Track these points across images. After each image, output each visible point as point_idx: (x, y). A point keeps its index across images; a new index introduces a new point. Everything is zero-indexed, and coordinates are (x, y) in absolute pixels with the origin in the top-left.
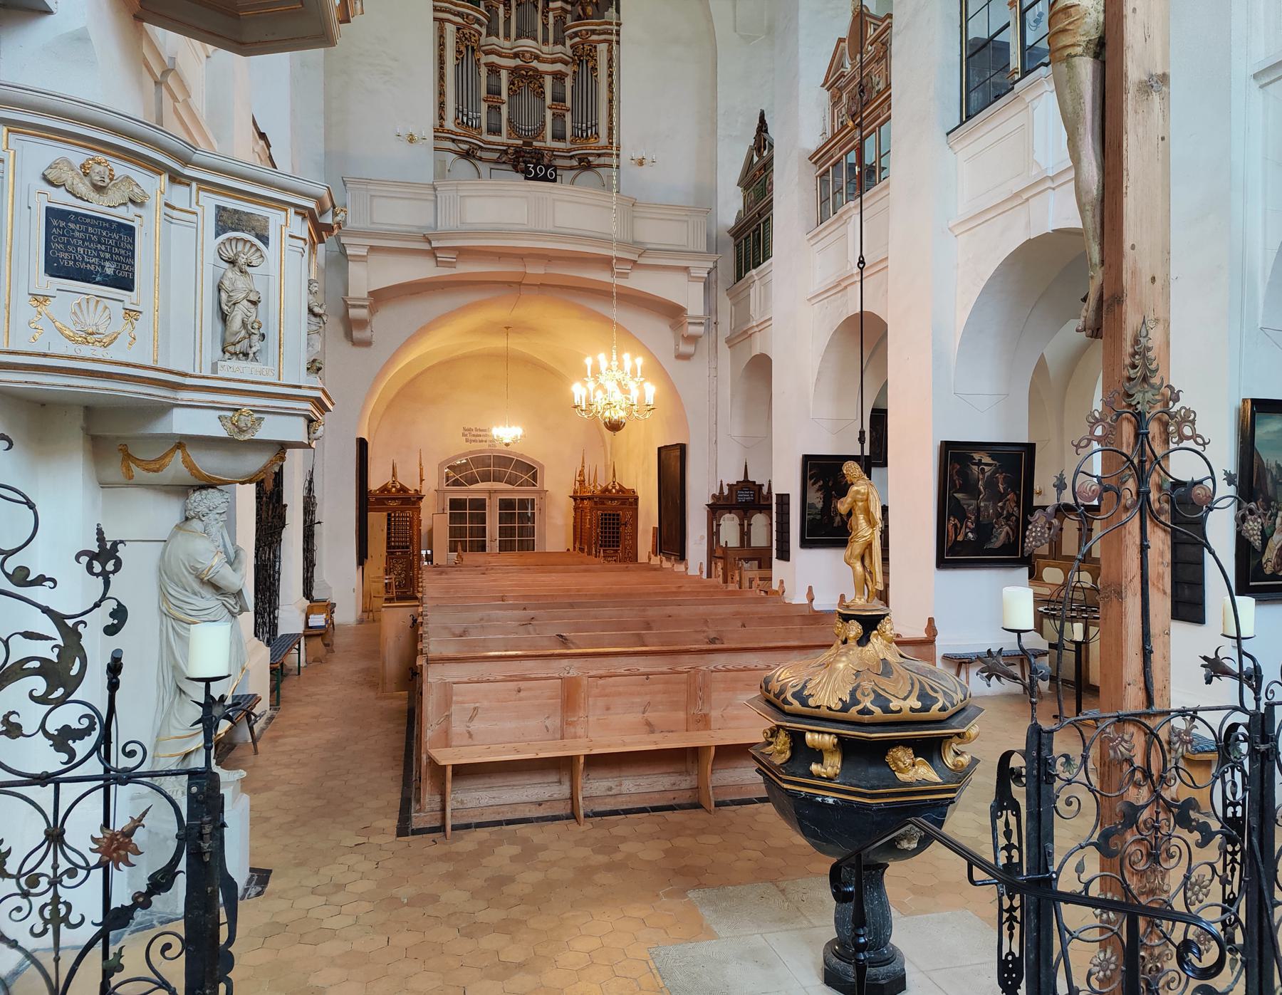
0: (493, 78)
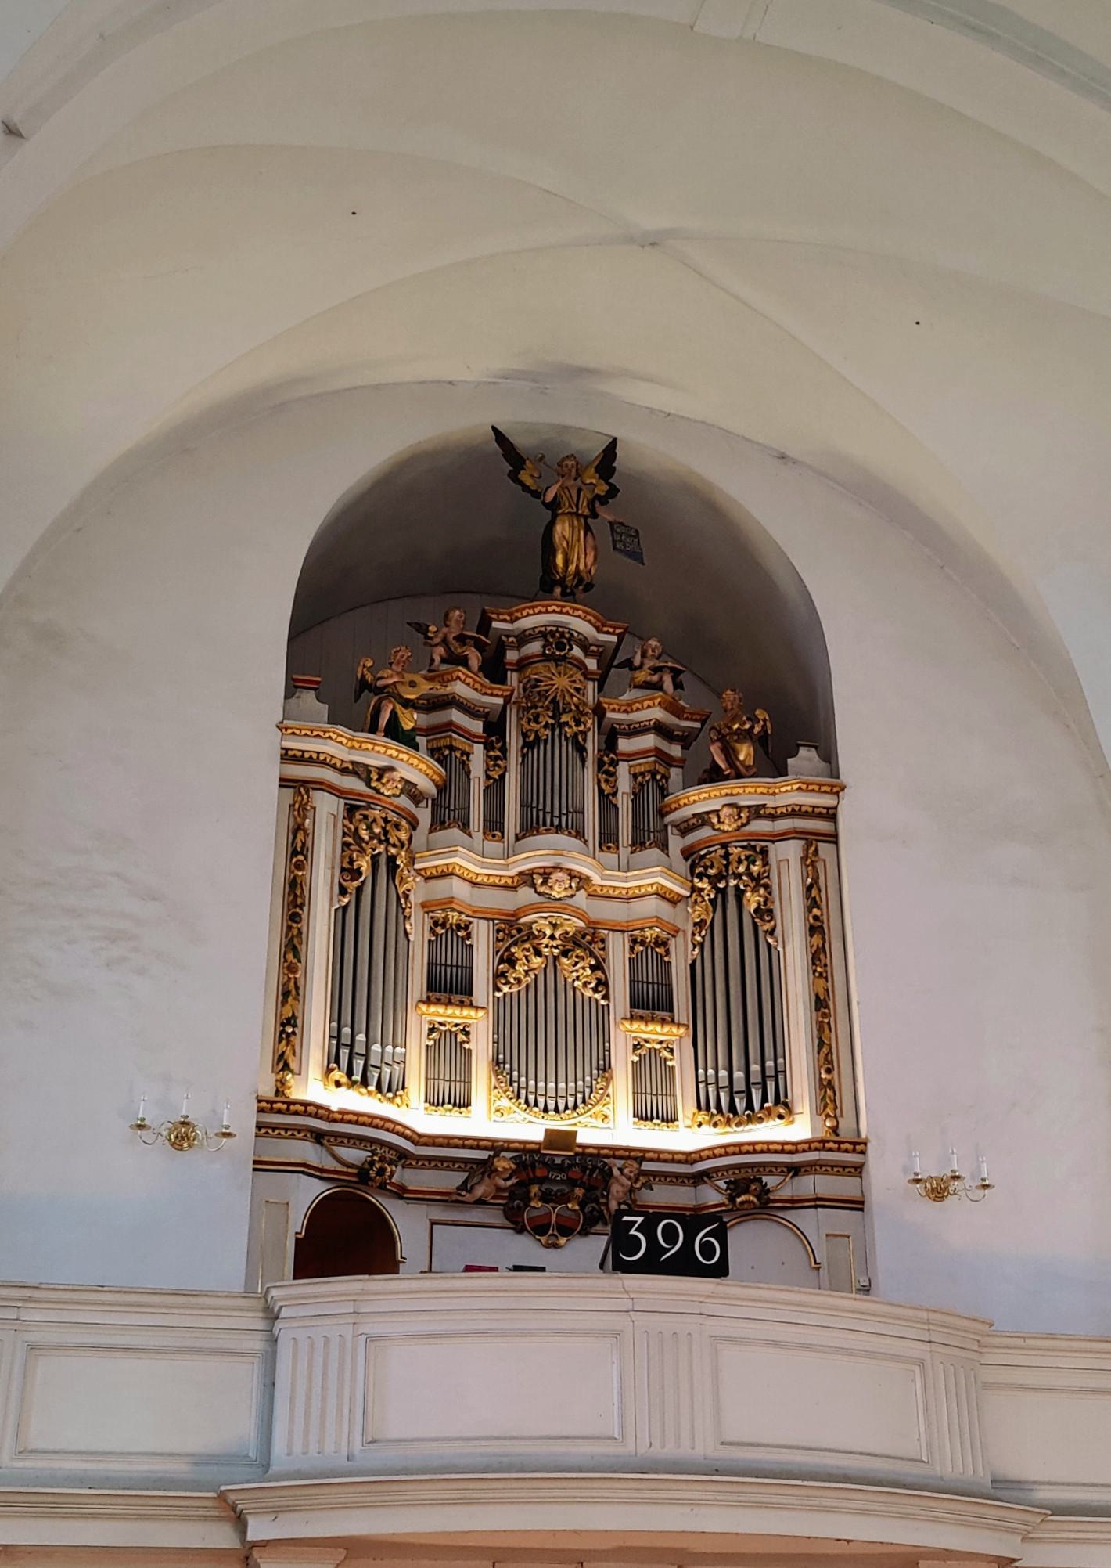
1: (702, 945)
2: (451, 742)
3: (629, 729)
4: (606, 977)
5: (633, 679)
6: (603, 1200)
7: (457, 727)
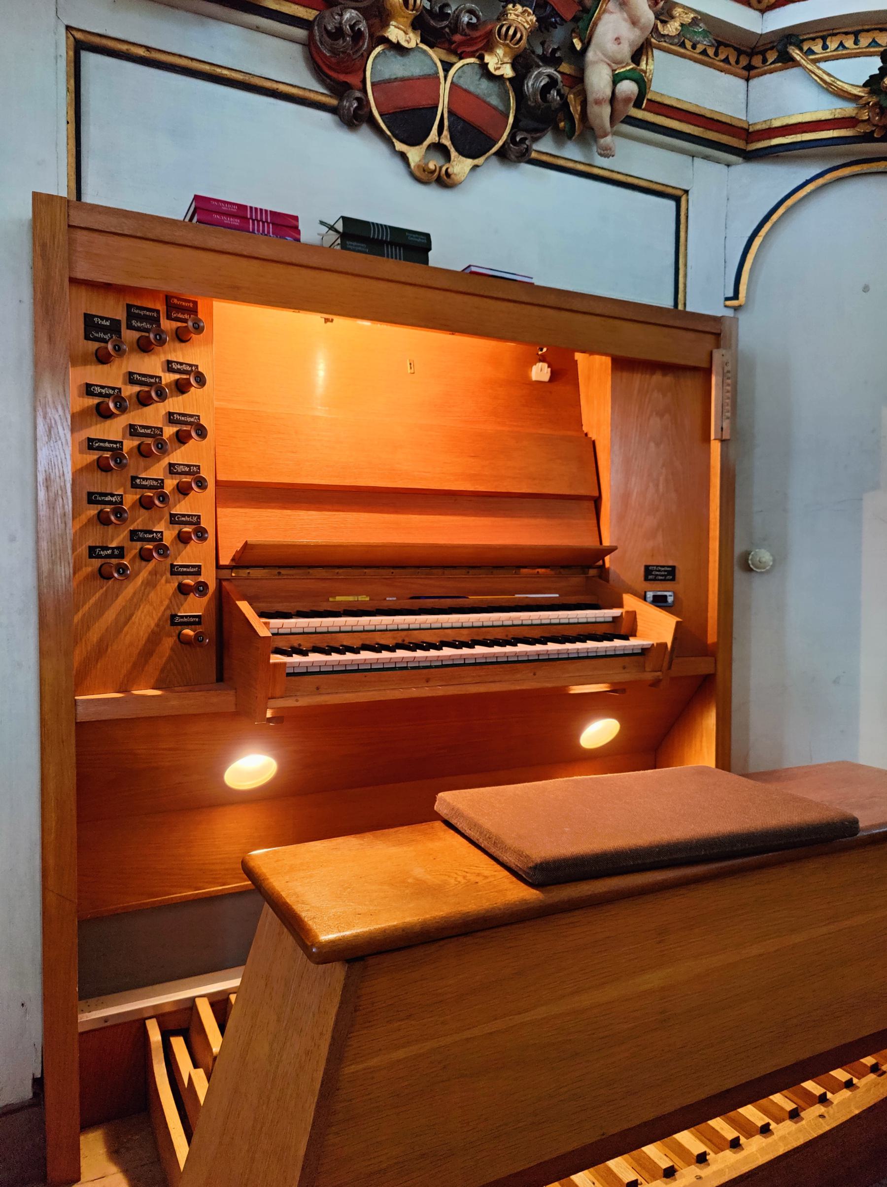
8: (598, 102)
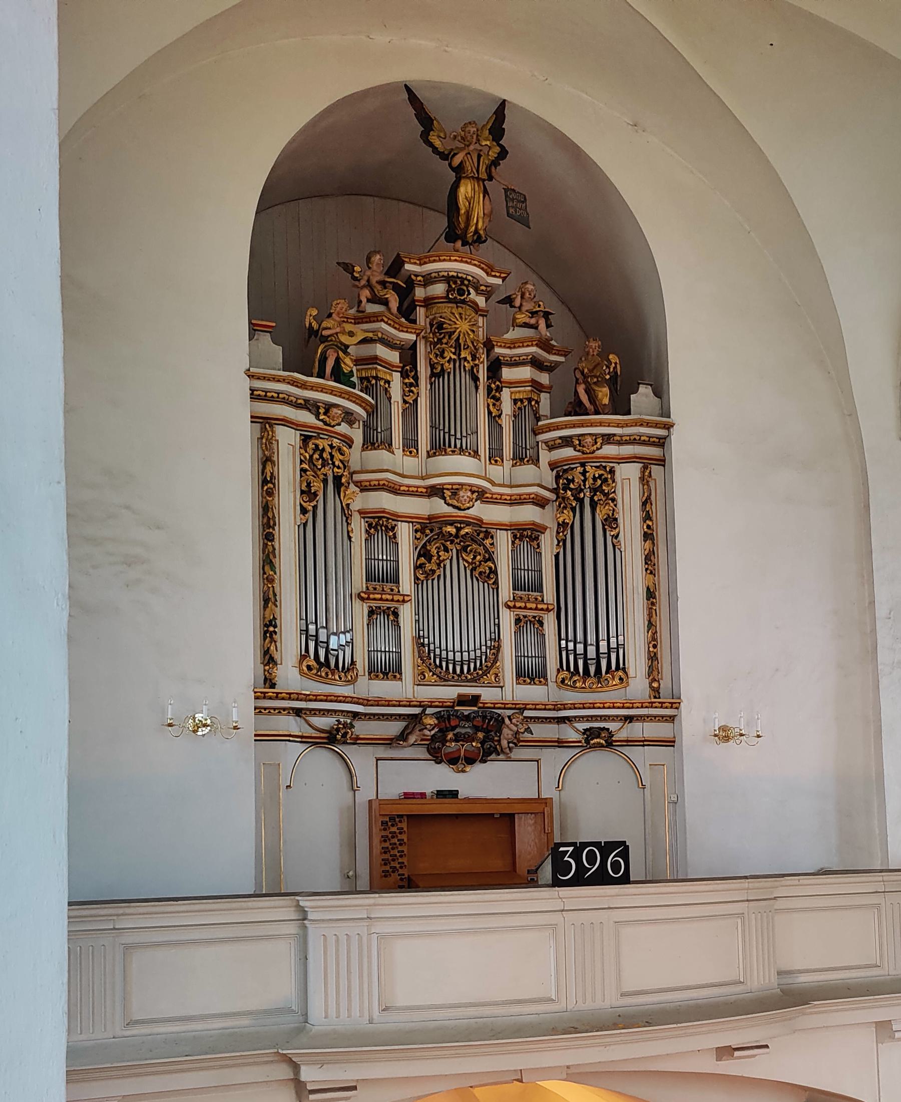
0: (380, 539)
1: (564, 541)
2: (376, 374)
3: (511, 360)
4: (495, 566)
5: (514, 319)
6: (496, 738)
7: (381, 360)
8: (506, 748)
